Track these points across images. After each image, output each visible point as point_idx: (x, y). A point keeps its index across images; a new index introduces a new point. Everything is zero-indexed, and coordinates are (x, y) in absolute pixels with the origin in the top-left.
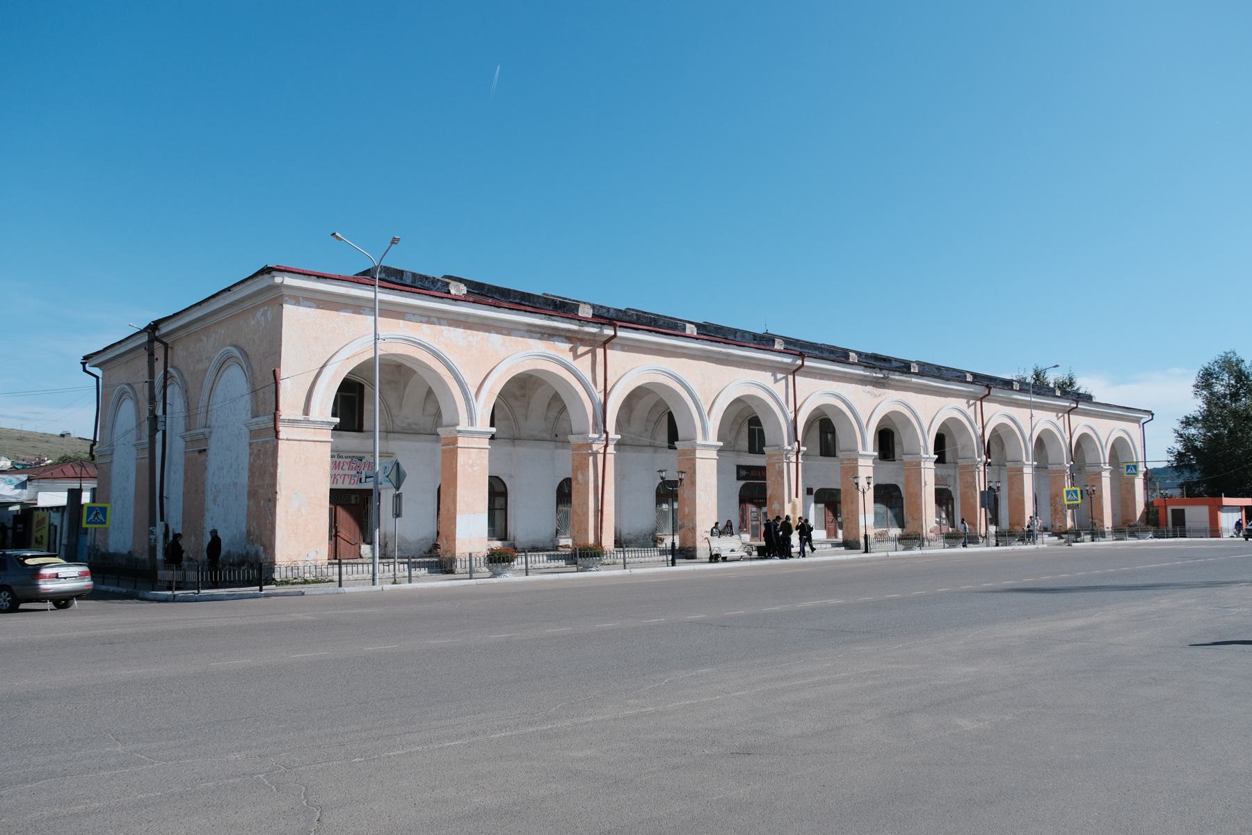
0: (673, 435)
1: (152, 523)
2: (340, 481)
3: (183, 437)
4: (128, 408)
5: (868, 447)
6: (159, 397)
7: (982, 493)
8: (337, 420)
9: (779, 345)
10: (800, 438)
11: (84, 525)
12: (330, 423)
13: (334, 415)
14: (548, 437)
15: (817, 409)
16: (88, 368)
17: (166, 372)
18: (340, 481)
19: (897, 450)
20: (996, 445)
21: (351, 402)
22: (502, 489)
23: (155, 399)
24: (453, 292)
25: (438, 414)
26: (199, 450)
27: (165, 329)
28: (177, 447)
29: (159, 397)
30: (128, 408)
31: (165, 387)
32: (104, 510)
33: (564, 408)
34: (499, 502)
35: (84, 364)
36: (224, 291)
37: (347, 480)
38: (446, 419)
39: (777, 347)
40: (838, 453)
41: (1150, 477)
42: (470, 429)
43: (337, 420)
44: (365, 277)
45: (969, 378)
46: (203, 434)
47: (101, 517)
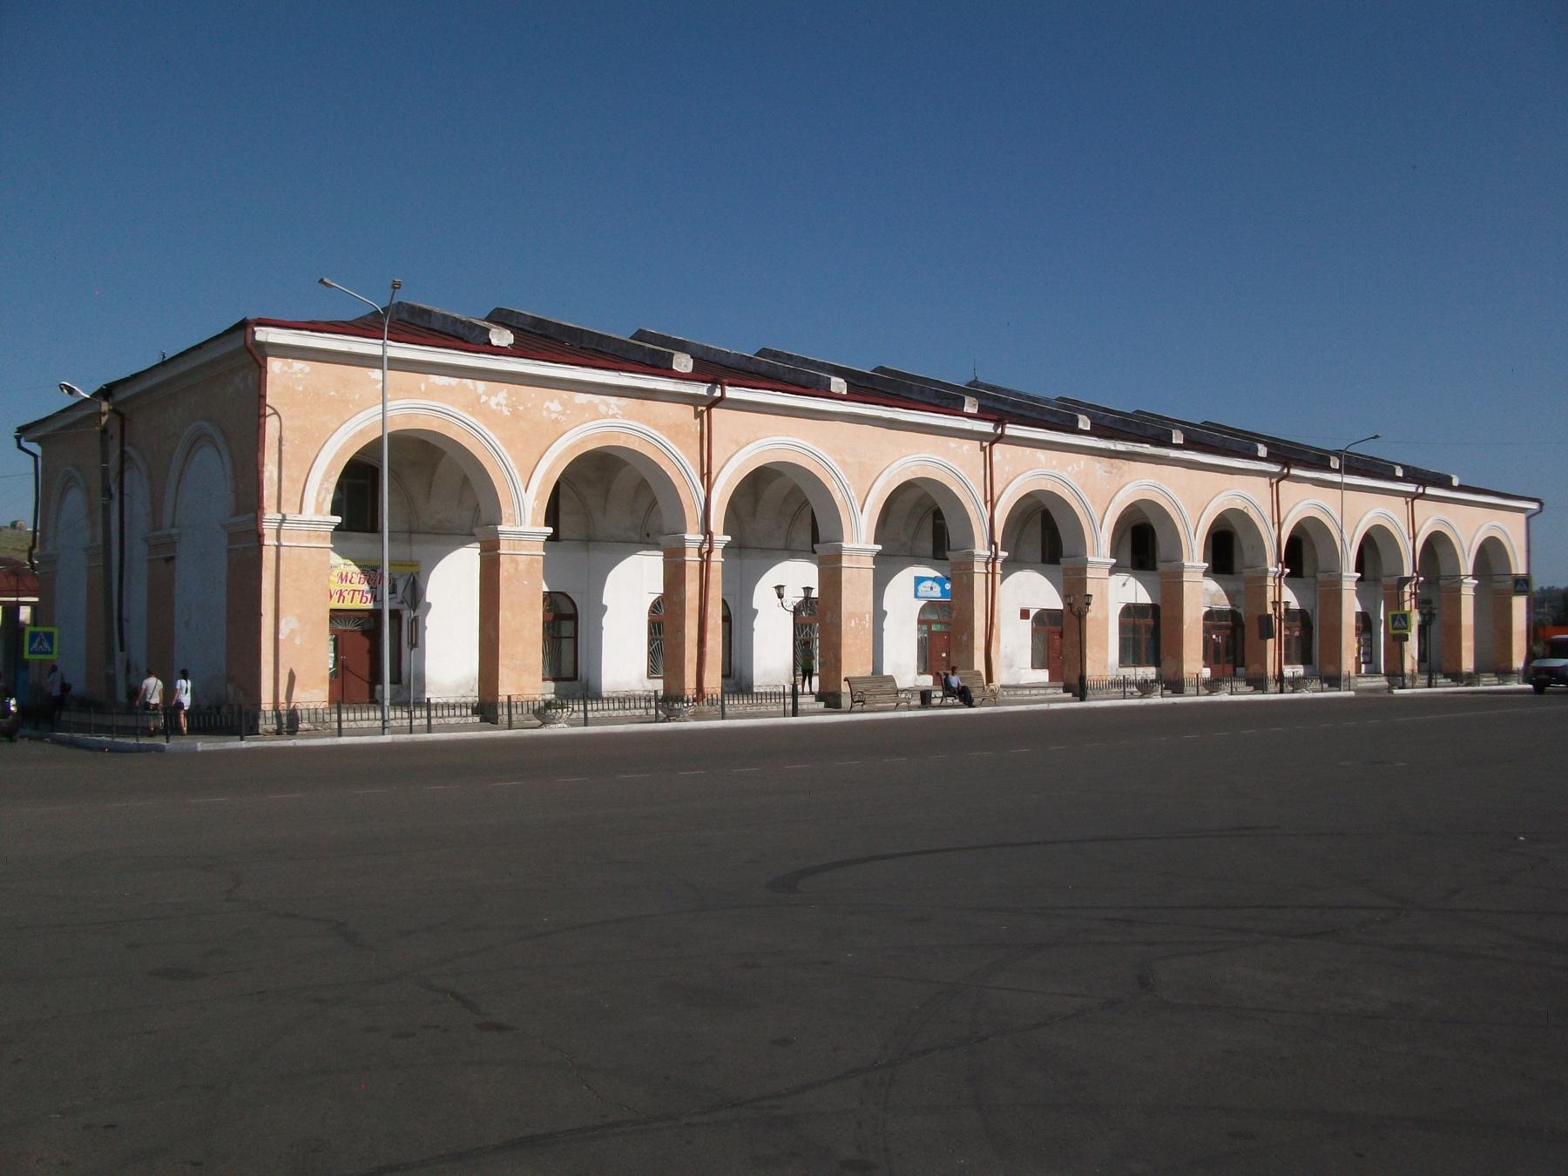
0: (815, 538)
1: (110, 657)
2: (348, 598)
3: (146, 540)
4: (76, 497)
5: (1194, 556)
6: (115, 489)
7: (187, 714)
8: (338, 519)
9: (970, 407)
10: (998, 539)
11: (27, 656)
12: (330, 523)
13: (334, 513)
14: (637, 538)
15: (1028, 496)
16: (24, 444)
17: (123, 452)
18: (348, 598)
19: (1237, 561)
20: (1304, 550)
21: (357, 492)
22: (570, 611)
23: (111, 491)
24: (495, 342)
25: (477, 509)
26: (165, 555)
27: (120, 395)
28: (138, 552)
29: (115, 489)
30: (76, 497)
31: (122, 473)
32: (49, 637)
33: (654, 502)
34: (566, 628)
35: (18, 439)
36: (194, 348)
37: (357, 596)
38: (484, 517)
39: (968, 409)
40: (1159, 565)
41: (187, 714)
42: (300, 517)
43: (338, 519)
44: (366, 327)
45: (1399, 473)
46: (169, 536)
47: (46, 644)
